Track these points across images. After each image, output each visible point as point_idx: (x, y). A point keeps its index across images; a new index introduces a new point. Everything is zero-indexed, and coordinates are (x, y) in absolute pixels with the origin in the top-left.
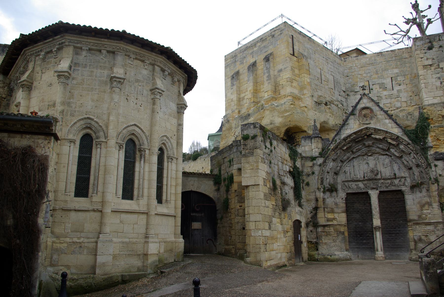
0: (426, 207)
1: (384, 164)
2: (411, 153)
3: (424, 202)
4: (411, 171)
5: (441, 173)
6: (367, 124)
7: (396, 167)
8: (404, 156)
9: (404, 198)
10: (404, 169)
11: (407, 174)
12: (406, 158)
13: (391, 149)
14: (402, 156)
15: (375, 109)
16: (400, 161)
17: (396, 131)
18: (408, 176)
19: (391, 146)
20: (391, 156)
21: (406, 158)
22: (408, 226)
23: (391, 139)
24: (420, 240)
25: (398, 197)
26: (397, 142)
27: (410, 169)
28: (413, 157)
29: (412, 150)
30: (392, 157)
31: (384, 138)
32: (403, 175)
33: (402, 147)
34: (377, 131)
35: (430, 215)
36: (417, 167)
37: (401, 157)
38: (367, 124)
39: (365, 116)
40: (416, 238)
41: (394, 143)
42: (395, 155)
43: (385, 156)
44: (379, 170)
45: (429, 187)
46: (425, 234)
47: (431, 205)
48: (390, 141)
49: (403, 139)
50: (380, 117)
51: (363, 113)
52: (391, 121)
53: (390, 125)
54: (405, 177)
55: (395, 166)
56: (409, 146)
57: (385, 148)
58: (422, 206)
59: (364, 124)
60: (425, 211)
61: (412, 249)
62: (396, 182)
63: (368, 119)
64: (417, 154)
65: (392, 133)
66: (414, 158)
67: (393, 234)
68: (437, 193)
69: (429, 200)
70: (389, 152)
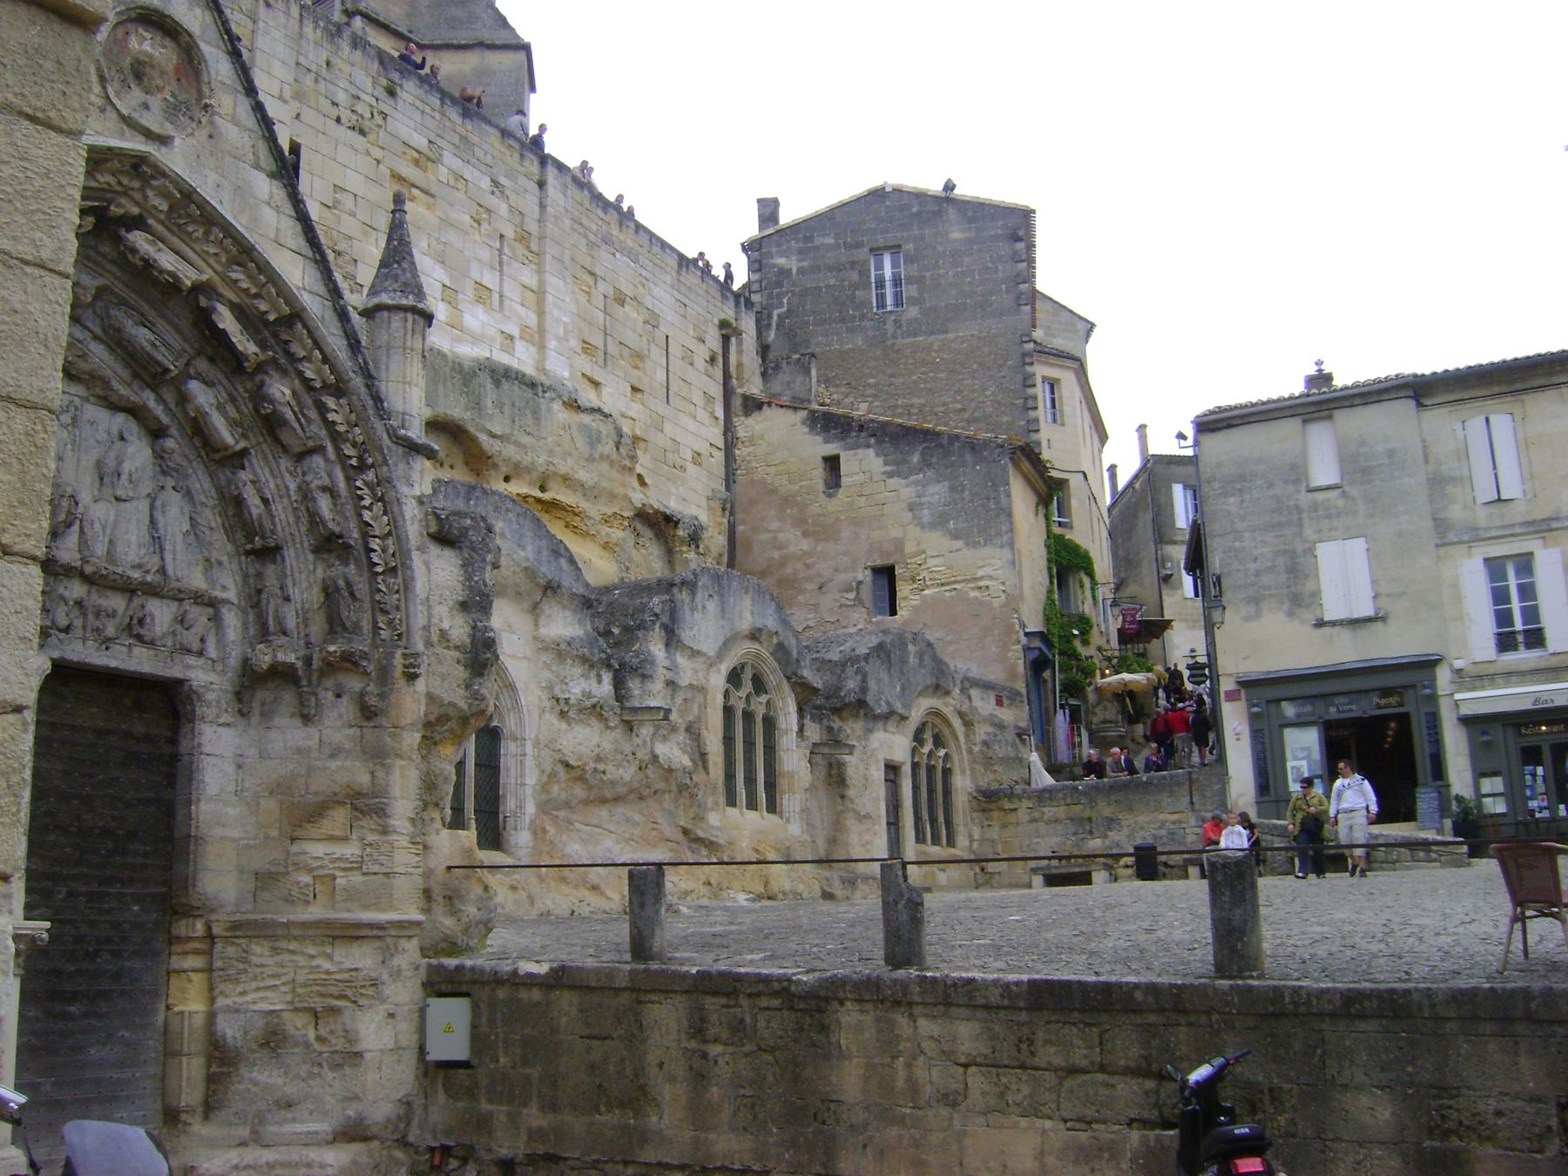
0: (338, 819)
1: (106, 475)
2: (320, 449)
3: (320, 785)
4: (270, 571)
5: (446, 625)
6: (149, 135)
7: (175, 518)
8: (255, 459)
9: (174, 741)
10: (221, 547)
11: (229, 587)
12: (265, 474)
13: (194, 386)
14: (244, 453)
15: (219, 66)
16: (207, 485)
17: (295, 272)
18: (231, 595)
19: (202, 365)
20: (156, 433)
21: (265, 474)
22: (172, 940)
23: (240, 312)
24: (273, 1040)
25: (139, 729)
26: (263, 345)
27: (269, 553)
28: (327, 482)
29: (336, 437)
30: (170, 443)
31: (198, 288)
32: (197, 581)
33: (280, 390)
34: (191, 214)
35: (357, 878)
36: (316, 551)
37: (238, 459)
38: (149, 135)
39: (139, 71)
40: (229, 1028)
41: (246, 346)
42: (198, 430)
43: (121, 419)
44: (80, 509)
45: (382, 696)
46: (317, 1002)
47: (381, 812)
48: (226, 321)
49: (317, 345)
50: (230, 132)
51: (134, 43)
52: (279, 194)
53: (269, 215)
54: (213, 604)
55: (173, 511)
56: (331, 402)
57: (164, 357)
58: (304, 815)
59: (126, 120)
60: (318, 850)
61: (190, 1110)
62: (161, 614)
63: (155, 102)
64: (362, 467)
65: (274, 278)
66: (330, 490)
67: (74, 997)
68: (418, 736)
69: (364, 779)
70: (161, 400)
